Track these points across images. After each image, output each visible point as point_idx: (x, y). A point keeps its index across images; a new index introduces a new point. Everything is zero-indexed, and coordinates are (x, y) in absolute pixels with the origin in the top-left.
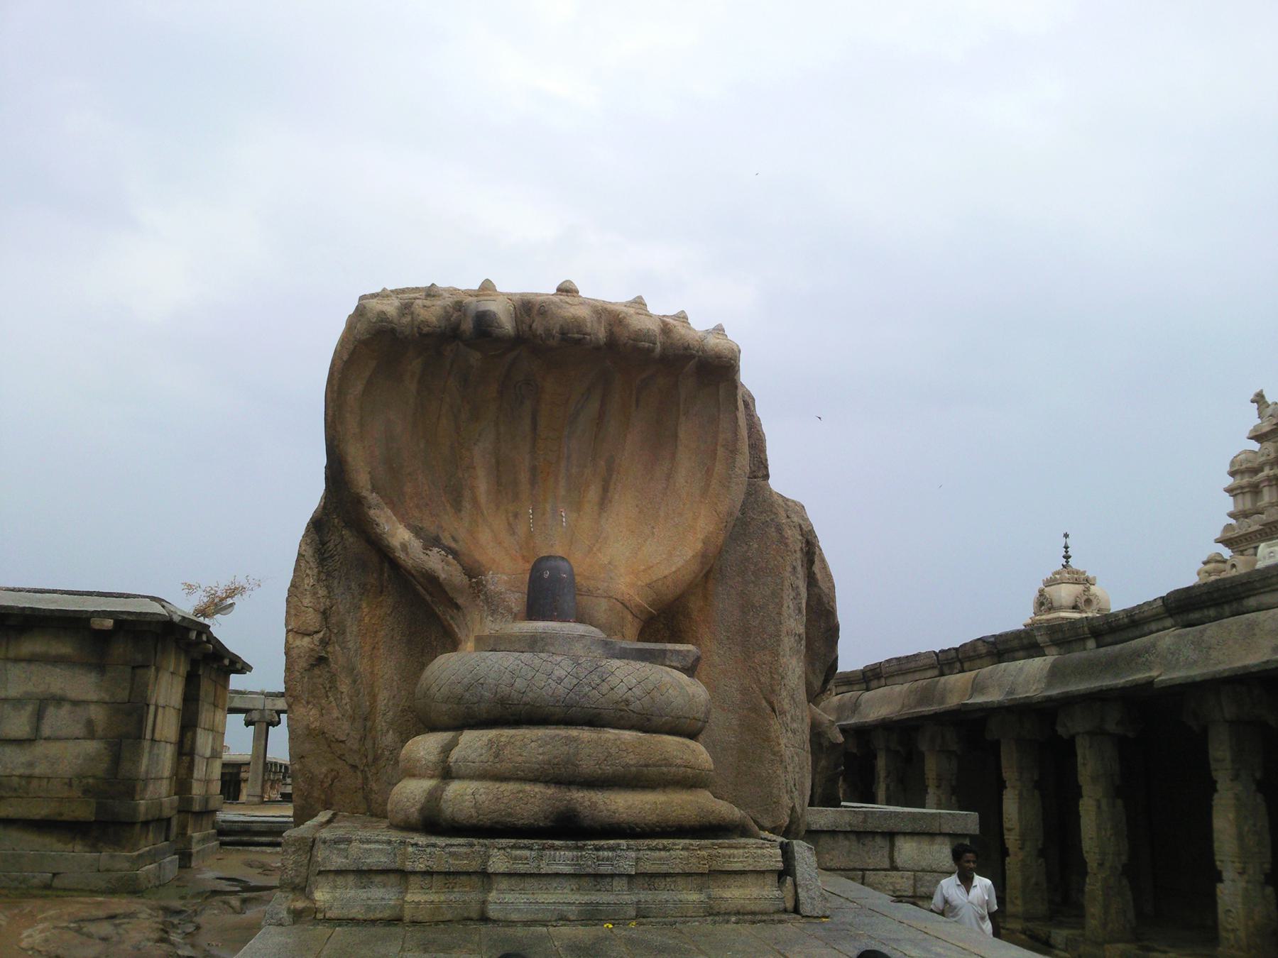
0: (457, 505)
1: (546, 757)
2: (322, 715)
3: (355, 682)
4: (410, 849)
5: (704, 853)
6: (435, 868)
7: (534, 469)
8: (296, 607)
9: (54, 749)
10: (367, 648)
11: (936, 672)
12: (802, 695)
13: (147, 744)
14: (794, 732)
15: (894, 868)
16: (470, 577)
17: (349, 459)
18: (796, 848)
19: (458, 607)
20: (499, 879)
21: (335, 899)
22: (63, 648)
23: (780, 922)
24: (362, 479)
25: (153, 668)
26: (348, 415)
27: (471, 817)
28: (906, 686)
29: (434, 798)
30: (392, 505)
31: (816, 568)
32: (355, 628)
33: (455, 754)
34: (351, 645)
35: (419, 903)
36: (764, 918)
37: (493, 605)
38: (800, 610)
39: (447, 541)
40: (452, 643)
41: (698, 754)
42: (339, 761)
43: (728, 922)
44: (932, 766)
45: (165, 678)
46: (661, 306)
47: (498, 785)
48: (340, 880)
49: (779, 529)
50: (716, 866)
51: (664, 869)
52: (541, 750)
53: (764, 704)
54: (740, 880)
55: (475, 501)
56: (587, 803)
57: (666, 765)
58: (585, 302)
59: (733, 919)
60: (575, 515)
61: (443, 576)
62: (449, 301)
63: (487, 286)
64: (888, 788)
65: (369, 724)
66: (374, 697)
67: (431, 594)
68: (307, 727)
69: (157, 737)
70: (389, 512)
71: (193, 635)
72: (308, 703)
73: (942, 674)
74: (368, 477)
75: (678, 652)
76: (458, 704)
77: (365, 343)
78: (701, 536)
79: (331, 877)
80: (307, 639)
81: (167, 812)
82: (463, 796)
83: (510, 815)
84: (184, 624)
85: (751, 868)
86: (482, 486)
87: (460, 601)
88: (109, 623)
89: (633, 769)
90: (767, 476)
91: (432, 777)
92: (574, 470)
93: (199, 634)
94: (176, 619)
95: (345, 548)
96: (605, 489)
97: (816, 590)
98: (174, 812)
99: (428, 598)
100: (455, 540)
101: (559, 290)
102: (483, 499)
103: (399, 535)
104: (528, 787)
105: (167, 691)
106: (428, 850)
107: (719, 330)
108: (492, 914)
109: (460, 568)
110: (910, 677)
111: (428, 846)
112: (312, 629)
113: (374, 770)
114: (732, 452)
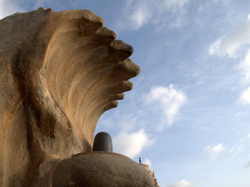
0: (62, 95)
19: (53, 137)
55: (67, 98)
87: (57, 134)
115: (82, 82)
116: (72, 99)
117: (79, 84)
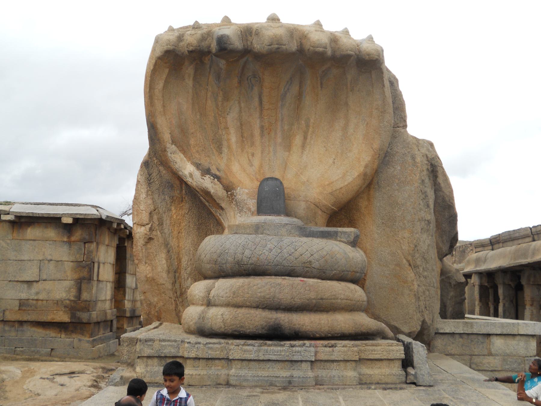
1: (262, 294)
2: (153, 270)
3: (169, 251)
4: (186, 345)
5: (356, 349)
6: (200, 356)
7: (262, 127)
8: (137, 211)
9: (48, 285)
10: (176, 232)
11: (531, 239)
12: (433, 254)
13: (95, 283)
14: (425, 277)
15: (490, 354)
16: (227, 191)
17: (159, 126)
18: (414, 346)
19: (222, 209)
20: (236, 362)
21: (147, 372)
22: (51, 233)
23: (401, 389)
24: (166, 136)
25: (95, 244)
26: (156, 101)
27: (221, 327)
28: (514, 247)
29: (202, 317)
30: (184, 152)
31: (440, 180)
32: (168, 222)
33: (213, 293)
34: (166, 231)
35: (192, 375)
36: (393, 386)
37: (240, 207)
38: (428, 206)
39: (214, 171)
40: (219, 228)
41: (355, 292)
42: (163, 295)
43: (370, 388)
44: (528, 293)
45: (102, 249)
46: (332, 26)
47: (235, 309)
48: (150, 361)
49: (413, 158)
50: (363, 356)
51: (333, 358)
52: (259, 290)
53: (405, 261)
54: (379, 364)
55: (229, 147)
56: (287, 320)
57: (334, 299)
58: (282, 26)
59: (373, 387)
60: (287, 153)
61: (212, 191)
62: (205, 31)
63: (226, 20)
64: (504, 305)
65: (177, 275)
66: (179, 261)
67: (208, 202)
68: (146, 276)
69: (101, 278)
70: (182, 156)
71: (115, 226)
72: (146, 263)
73: (534, 240)
74: (169, 136)
75: (345, 233)
76: (215, 264)
77: (160, 58)
78: (363, 164)
79: (145, 359)
80: (143, 228)
81: (109, 317)
82: (218, 317)
83: (242, 327)
84: (108, 220)
85: (385, 357)
86: (233, 139)
87: (223, 205)
88: (70, 221)
89: (314, 301)
90: (405, 126)
91: (202, 305)
92: (286, 127)
93: (119, 224)
94: (104, 217)
95: (161, 177)
96: (305, 138)
97: (441, 193)
98: (115, 317)
99: (207, 204)
100: (218, 170)
101: (268, 19)
102: (234, 146)
103: (188, 170)
104: (253, 311)
105: (106, 255)
106: (196, 346)
107: (370, 39)
108: (232, 382)
109: (221, 186)
110: (516, 242)
111: (196, 343)
112: (145, 223)
113: (180, 300)
114: (382, 112)
115: (243, 105)
116: (242, 136)
117: (240, 111)
